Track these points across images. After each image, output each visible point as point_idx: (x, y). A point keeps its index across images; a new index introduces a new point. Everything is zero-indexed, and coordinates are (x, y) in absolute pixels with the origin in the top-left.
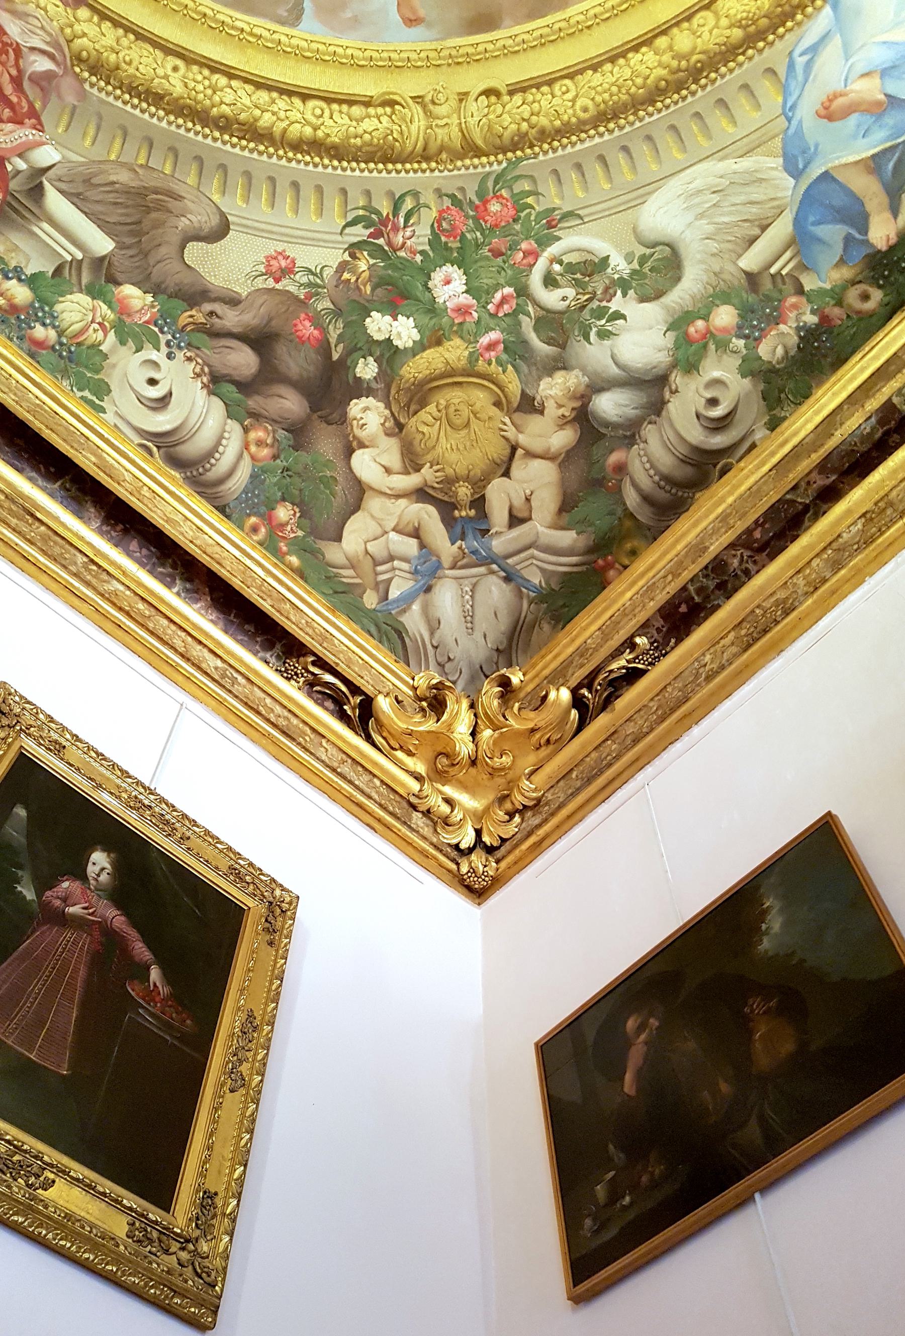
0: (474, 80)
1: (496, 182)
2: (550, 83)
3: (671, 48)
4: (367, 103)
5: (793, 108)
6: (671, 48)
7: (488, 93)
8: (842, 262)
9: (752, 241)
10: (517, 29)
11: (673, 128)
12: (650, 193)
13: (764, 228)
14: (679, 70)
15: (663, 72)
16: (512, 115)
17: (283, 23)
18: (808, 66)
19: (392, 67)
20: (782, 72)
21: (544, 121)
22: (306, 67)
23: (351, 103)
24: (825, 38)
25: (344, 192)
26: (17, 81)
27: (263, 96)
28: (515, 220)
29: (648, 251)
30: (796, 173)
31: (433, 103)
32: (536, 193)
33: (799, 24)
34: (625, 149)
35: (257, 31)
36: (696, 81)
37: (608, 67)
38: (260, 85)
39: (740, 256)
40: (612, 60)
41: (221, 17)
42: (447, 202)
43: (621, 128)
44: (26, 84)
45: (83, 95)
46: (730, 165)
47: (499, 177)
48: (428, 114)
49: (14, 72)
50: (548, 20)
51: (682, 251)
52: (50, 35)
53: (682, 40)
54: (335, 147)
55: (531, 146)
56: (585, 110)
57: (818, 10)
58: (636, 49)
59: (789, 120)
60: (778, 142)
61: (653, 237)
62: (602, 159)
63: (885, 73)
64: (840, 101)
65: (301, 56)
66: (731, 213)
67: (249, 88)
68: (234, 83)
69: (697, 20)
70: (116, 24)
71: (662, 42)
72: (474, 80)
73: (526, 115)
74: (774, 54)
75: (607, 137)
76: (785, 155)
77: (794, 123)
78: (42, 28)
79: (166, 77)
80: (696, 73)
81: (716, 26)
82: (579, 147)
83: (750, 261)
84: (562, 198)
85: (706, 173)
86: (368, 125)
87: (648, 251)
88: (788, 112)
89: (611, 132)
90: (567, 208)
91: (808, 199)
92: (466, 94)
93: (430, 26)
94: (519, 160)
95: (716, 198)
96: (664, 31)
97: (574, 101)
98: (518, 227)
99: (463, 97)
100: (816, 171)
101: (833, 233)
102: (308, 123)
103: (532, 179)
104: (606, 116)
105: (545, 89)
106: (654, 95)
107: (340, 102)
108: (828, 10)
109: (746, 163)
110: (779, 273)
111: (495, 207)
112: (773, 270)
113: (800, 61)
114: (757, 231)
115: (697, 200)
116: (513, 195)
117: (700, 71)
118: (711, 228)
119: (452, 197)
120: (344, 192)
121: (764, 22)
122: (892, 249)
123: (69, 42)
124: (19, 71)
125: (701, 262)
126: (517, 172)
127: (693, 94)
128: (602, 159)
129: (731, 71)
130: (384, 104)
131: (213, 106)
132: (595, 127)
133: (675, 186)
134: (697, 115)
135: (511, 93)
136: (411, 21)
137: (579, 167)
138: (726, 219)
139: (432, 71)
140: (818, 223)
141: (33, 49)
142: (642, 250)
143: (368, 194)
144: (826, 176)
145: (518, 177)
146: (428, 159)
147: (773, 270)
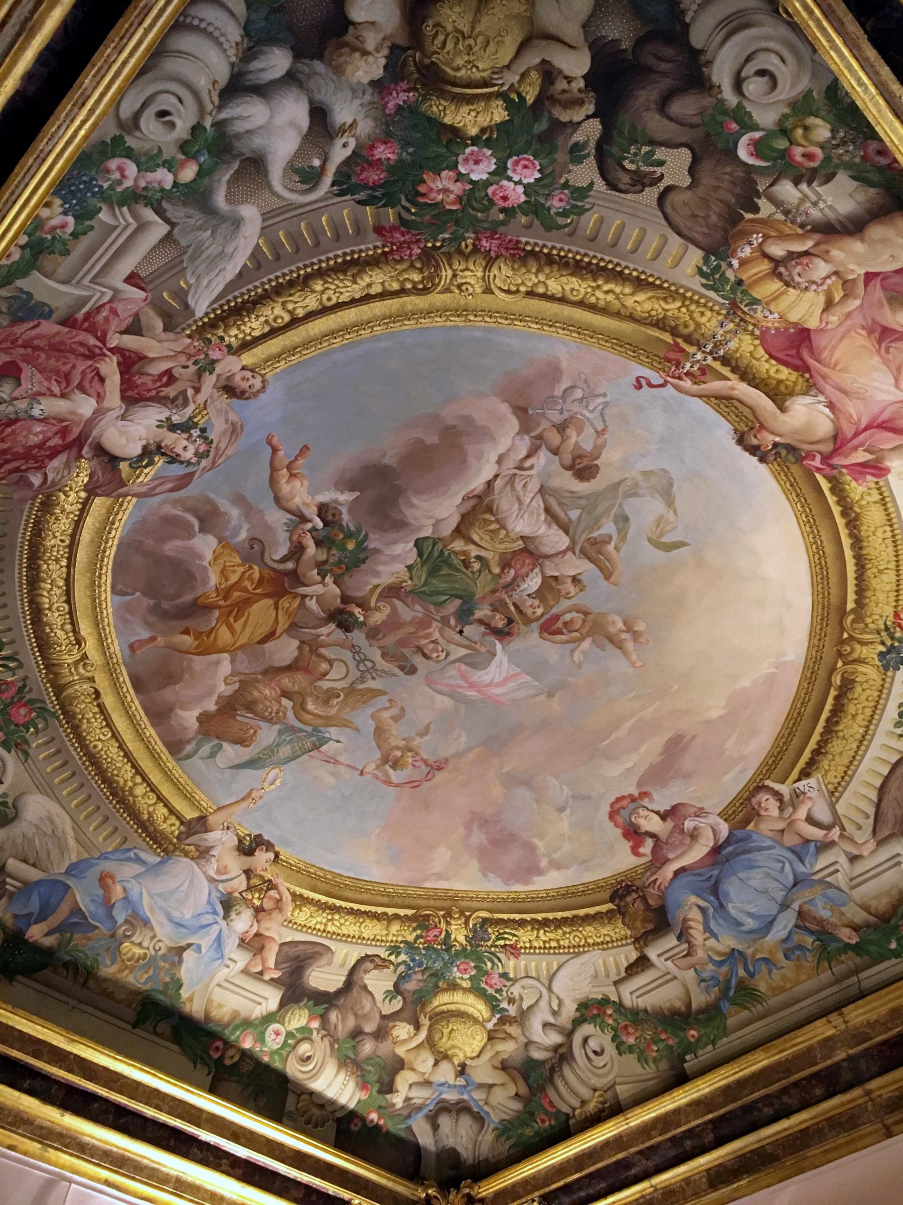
0: (102, 683)
1: (39, 708)
2: (108, 725)
3: (135, 784)
4: (75, 631)
5: (106, 858)
6: (135, 784)
7: (97, 694)
8: (16, 917)
9: (25, 861)
10: (137, 702)
11: (90, 797)
12: (48, 795)
13: (34, 865)
14: (123, 792)
15: (122, 784)
16: (86, 709)
17: (113, 587)
18: (129, 859)
19: (101, 641)
20: (125, 846)
21: (85, 726)
22: (88, 601)
23: (73, 623)
24: (143, 863)
25: (10, 630)
26: (17, 470)
27: (61, 583)
28: (16, 725)
29: (10, 805)
30: (68, 872)
31: (85, 664)
32: (37, 731)
33: (151, 847)
34: (74, 774)
35: (103, 577)
36: (118, 802)
37: (122, 754)
38: (69, 581)
39: (15, 857)
40: (126, 755)
41: (106, 560)
42: (20, 684)
43: (86, 769)
44: (18, 474)
45: (23, 501)
46: (70, 834)
47: (45, 709)
48: (76, 663)
49: (23, 468)
50: (145, 719)
51: (12, 825)
52: (60, 480)
53: (140, 790)
54: (40, 620)
55: (67, 723)
56: (95, 747)
57: (159, 855)
58: (133, 766)
59: (99, 858)
60: (86, 856)
61: (20, 805)
62: (65, 763)
63: (126, 899)
64: (109, 881)
65: (95, 600)
66: (40, 843)
67: (64, 575)
68: (64, 569)
69: (151, 795)
70: (82, 511)
71: (138, 779)
72: (102, 683)
73: (87, 716)
74: (136, 838)
75: (80, 762)
76: (78, 862)
77: (96, 861)
78: (63, 477)
79: (55, 537)
80: (122, 801)
81: (149, 806)
82: (71, 749)
83: (13, 865)
84: (37, 747)
85: (65, 823)
86: (60, 633)
87: (10, 805)
88: (104, 857)
89: (84, 764)
90: (30, 751)
91: (55, 882)
92: (94, 681)
93: (131, 657)
94: (58, 718)
95: (49, 832)
96: (145, 779)
97: (100, 740)
98: (12, 727)
99: (92, 680)
100: (70, 882)
101: (34, 904)
102: (51, 605)
103: (45, 729)
104: (93, 758)
105: (104, 723)
106: (108, 781)
107: (71, 618)
108: (159, 859)
109: (72, 843)
110: (6, 883)
111: (23, 711)
112: (8, 880)
113: (132, 854)
114: (31, 862)
115: (47, 822)
116: (33, 720)
117: (124, 803)
118: (30, 835)
119: (24, 686)
120: (10, 630)
121: (152, 829)
122: (26, 942)
123: (60, 490)
124: (25, 471)
125: (8, 837)
126: (49, 718)
127: (111, 802)
128: (65, 763)
129: (125, 819)
130: (76, 639)
131: (45, 561)
132: (85, 755)
133: (54, 808)
134: (98, 808)
135: (99, 705)
136: (132, 647)
137: (58, 751)
138: (37, 842)
139: (104, 661)
140: (39, 894)
141: (45, 474)
142: (10, 801)
143: (12, 642)
144: (67, 888)
145: (45, 720)
146: (47, 667)
147: (8, 880)
